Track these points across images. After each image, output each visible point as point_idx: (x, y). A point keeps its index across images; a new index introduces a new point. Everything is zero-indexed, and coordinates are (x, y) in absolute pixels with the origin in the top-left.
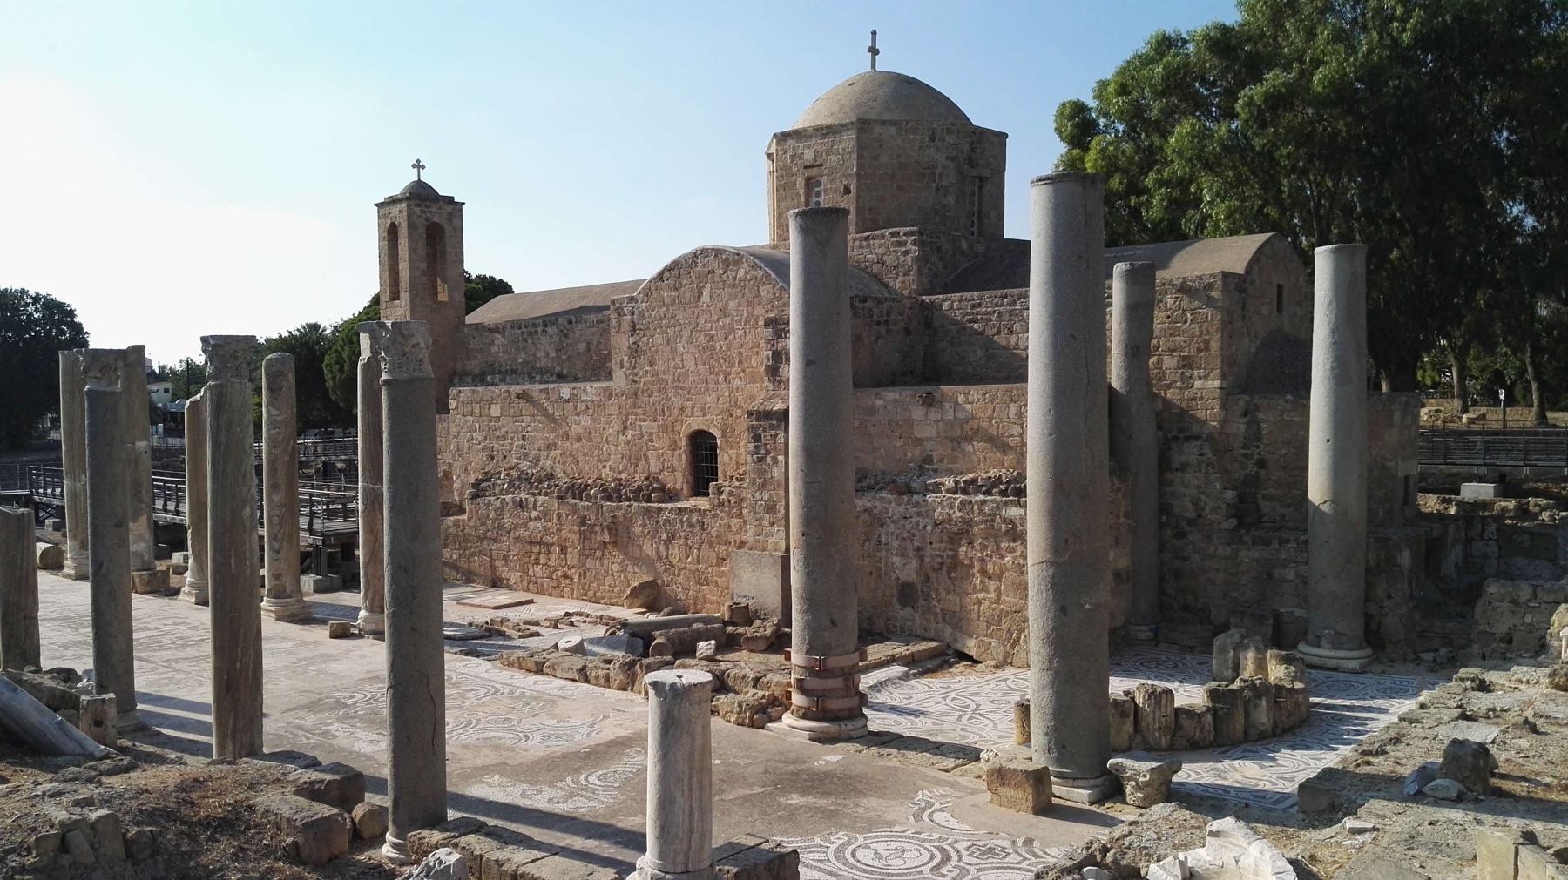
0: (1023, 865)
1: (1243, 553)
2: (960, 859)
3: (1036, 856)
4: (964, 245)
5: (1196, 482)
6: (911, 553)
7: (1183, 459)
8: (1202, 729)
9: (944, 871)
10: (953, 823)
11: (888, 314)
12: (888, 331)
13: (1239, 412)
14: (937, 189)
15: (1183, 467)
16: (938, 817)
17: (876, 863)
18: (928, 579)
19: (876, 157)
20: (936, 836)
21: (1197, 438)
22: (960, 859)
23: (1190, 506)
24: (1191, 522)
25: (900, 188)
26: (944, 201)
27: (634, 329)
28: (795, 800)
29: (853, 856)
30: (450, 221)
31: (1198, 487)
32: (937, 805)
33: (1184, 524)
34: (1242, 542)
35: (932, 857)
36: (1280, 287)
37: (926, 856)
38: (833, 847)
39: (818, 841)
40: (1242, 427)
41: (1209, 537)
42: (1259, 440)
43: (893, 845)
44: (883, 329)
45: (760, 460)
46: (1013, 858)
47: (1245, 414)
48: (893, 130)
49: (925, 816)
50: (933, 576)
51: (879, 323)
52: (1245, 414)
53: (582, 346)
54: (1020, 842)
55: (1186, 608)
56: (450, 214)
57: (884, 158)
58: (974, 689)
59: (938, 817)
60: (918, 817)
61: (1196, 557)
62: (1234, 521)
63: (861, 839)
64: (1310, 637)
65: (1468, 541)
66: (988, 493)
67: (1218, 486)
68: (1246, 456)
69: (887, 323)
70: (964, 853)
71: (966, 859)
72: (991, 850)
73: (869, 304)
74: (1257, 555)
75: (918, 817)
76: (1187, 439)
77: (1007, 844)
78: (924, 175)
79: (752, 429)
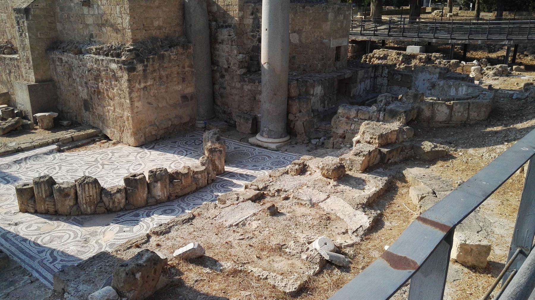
1: (245, 87)
5: (227, 50)
6: (84, 85)
13: (250, 13)
15: (222, 42)
18: (91, 99)
21: (230, 26)
24: (226, 70)
31: (228, 52)
34: (245, 81)
40: (251, 21)
41: (233, 78)
45: (21, 35)
47: (252, 14)
50: (93, 96)
52: (252, 14)
55: (224, 112)
61: (228, 88)
62: (243, 71)
65: (375, 77)
66: (107, 55)
67: (235, 52)
68: (253, 36)
76: (226, 27)
79: (16, 17)
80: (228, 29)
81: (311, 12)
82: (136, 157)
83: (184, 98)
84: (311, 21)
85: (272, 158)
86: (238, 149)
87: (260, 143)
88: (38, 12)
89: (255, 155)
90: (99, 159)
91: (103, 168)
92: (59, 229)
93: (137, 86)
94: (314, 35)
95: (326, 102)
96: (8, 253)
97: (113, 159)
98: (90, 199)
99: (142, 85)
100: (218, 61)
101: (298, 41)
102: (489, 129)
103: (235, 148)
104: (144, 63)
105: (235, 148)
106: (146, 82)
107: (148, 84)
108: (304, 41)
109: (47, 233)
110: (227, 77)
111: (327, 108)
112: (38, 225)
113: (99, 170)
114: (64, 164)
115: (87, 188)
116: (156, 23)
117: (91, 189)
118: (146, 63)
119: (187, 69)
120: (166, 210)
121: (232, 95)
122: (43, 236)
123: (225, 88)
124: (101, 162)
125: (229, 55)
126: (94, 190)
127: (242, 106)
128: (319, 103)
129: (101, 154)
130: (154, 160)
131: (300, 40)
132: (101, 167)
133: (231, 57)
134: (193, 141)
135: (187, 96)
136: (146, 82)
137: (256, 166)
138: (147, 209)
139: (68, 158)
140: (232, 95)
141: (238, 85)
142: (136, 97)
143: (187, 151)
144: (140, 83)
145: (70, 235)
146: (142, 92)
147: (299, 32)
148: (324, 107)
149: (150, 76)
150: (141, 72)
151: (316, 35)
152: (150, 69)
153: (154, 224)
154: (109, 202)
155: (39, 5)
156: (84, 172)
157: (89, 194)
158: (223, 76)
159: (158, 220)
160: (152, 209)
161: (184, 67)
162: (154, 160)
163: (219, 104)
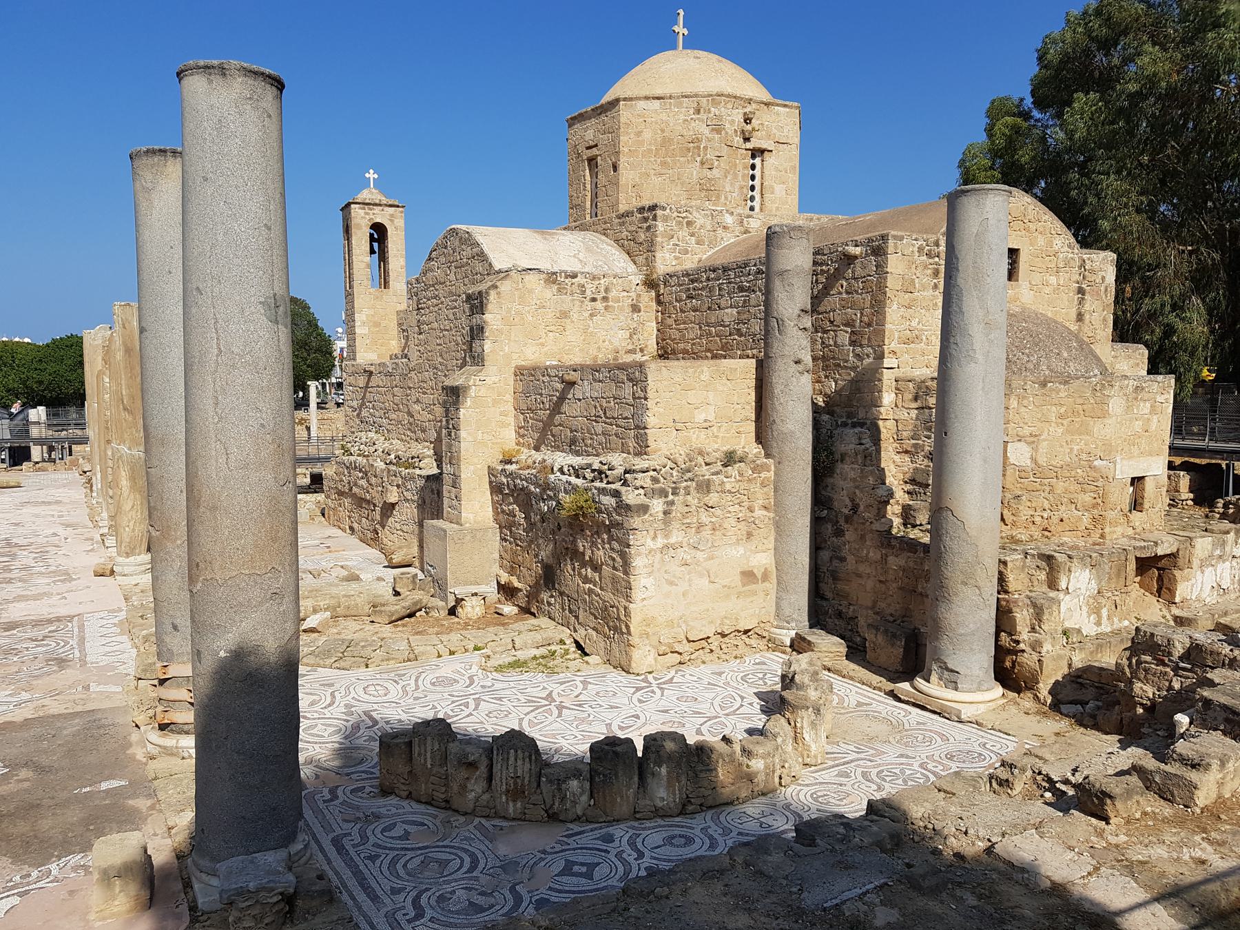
1: (891, 559)
4: (729, 220)
5: (852, 475)
8: (563, 799)
11: (607, 290)
12: (606, 308)
13: (910, 396)
14: (702, 163)
15: (843, 457)
19: (639, 134)
21: (862, 425)
23: (848, 502)
24: (848, 519)
25: (664, 164)
26: (709, 174)
30: (392, 221)
31: (854, 480)
36: (1013, 253)
40: (914, 413)
41: (863, 537)
44: (599, 305)
47: (916, 399)
51: (594, 300)
55: (840, 615)
56: (392, 215)
57: (647, 135)
68: (915, 446)
69: (605, 299)
76: (854, 425)
78: (689, 150)
80: (857, 430)
81: (1061, 395)
82: (630, 700)
83: (748, 576)
84: (1061, 417)
85: (952, 740)
86: (865, 708)
87: (922, 700)
88: (483, 392)
89: (907, 726)
90: (554, 695)
91: (560, 715)
92: (444, 843)
93: (650, 543)
94: (1072, 449)
95: (1104, 612)
96: (335, 881)
97: (581, 697)
98: (516, 783)
99: (660, 542)
100: (830, 499)
101: (1029, 462)
102: (104, 786)
103: (859, 704)
104: (666, 496)
105: (859, 704)
106: (667, 536)
107: (673, 540)
108: (1042, 460)
109: (419, 848)
110: (850, 535)
111: (1106, 628)
112: (407, 827)
113: (551, 719)
114: (486, 698)
115: (512, 759)
116: (700, 417)
117: (520, 762)
118: (671, 497)
119: (759, 513)
120: (673, 837)
121: (859, 576)
122: (410, 854)
123: (843, 559)
124: (558, 700)
125: (857, 487)
126: (527, 766)
127: (883, 605)
128: (1085, 614)
129: (562, 683)
130: (666, 711)
131: (1034, 460)
132: (556, 712)
133: (862, 492)
134: (761, 675)
135: (755, 571)
136: (667, 536)
137: (908, 757)
138: (633, 828)
139: (498, 685)
140: (859, 576)
141: (875, 555)
142: (645, 566)
143: (742, 698)
144: (655, 538)
145: (461, 858)
146: (659, 555)
147: (1033, 440)
148: (1098, 624)
149: (676, 524)
150: (661, 516)
151: (1076, 448)
152: (678, 509)
153: (643, 866)
154: (554, 796)
155: (487, 379)
156: (521, 720)
157: (516, 771)
158: (839, 533)
159: (653, 858)
160: (644, 829)
161: (751, 510)
162: (666, 711)
163: (829, 595)
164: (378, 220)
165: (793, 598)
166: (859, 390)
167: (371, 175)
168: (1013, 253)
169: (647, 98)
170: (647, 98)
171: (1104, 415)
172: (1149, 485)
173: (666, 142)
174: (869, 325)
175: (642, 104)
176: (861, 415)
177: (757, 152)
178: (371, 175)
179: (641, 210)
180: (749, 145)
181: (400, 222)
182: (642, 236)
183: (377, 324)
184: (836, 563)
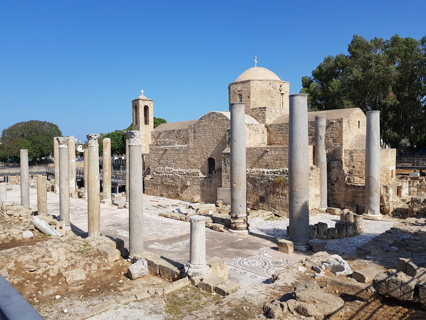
0: (285, 266)
2: (269, 264)
3: (288, 264)
4: (278, 111)
7: (333, 166)
8: (335, 234)
9: (265, 267)
10: (269, 256)
16: (265, 254)
17: (248, 265)
19: (255, 89)
20: (264, 259)
21: (337, 160)
22: (269, 264)
23: (335, 178)
24: (335, 182)
27: (194, 132)
28: (230, 249)
29: (243, 263)
31: (337, 173)
32: (265, 252)
33: (334, 182)
35: (263, 264)
37: (261, 263)
38: (238, 261)
39: (234, 259)
41: (340, 186)
42: (353, 161)
43: (253, 261)
44: (257, 132)
46: (283, 264)
47: (350, 154)
48: (260, 81)
49: (262, 254)
52: (350, 154)
53: (182, 137)
54: (285, 261)
57: (258, 89)
58: (278, 223)
59: (265, 254)
60: (260, 254)
61: (337, 191)
63: (245, 259)
64: (365, 211)
70: (271, 263)
71: (271, 264)
72: (275, 263)
73: (253, 126)
74: (352, 190)
75: (260, 254)
76: (334, 160)
77: (281, 261)
119: (317, 181)
121: (339, 194)
123: (334, 191)
127: (347, 200)
140: (339, 194)
164: (146, 105)
165: (324, 201)
166: (336, 152)
167: (142, 91)
168: (359, 121)
169: (258, 80)
170: (258, 80)
171: (387, 157)
172: (393, 171)
173: (262, 91)
174: (338, 138)
175: (256, 82)
176: (337, 158)
177: (282, 94)
178: (142, 91)
179: (260, 108)
180: (281, 93)
181: (152, 105)
182: (260, 115)
183: (146, 135)
184: (332, 192)
